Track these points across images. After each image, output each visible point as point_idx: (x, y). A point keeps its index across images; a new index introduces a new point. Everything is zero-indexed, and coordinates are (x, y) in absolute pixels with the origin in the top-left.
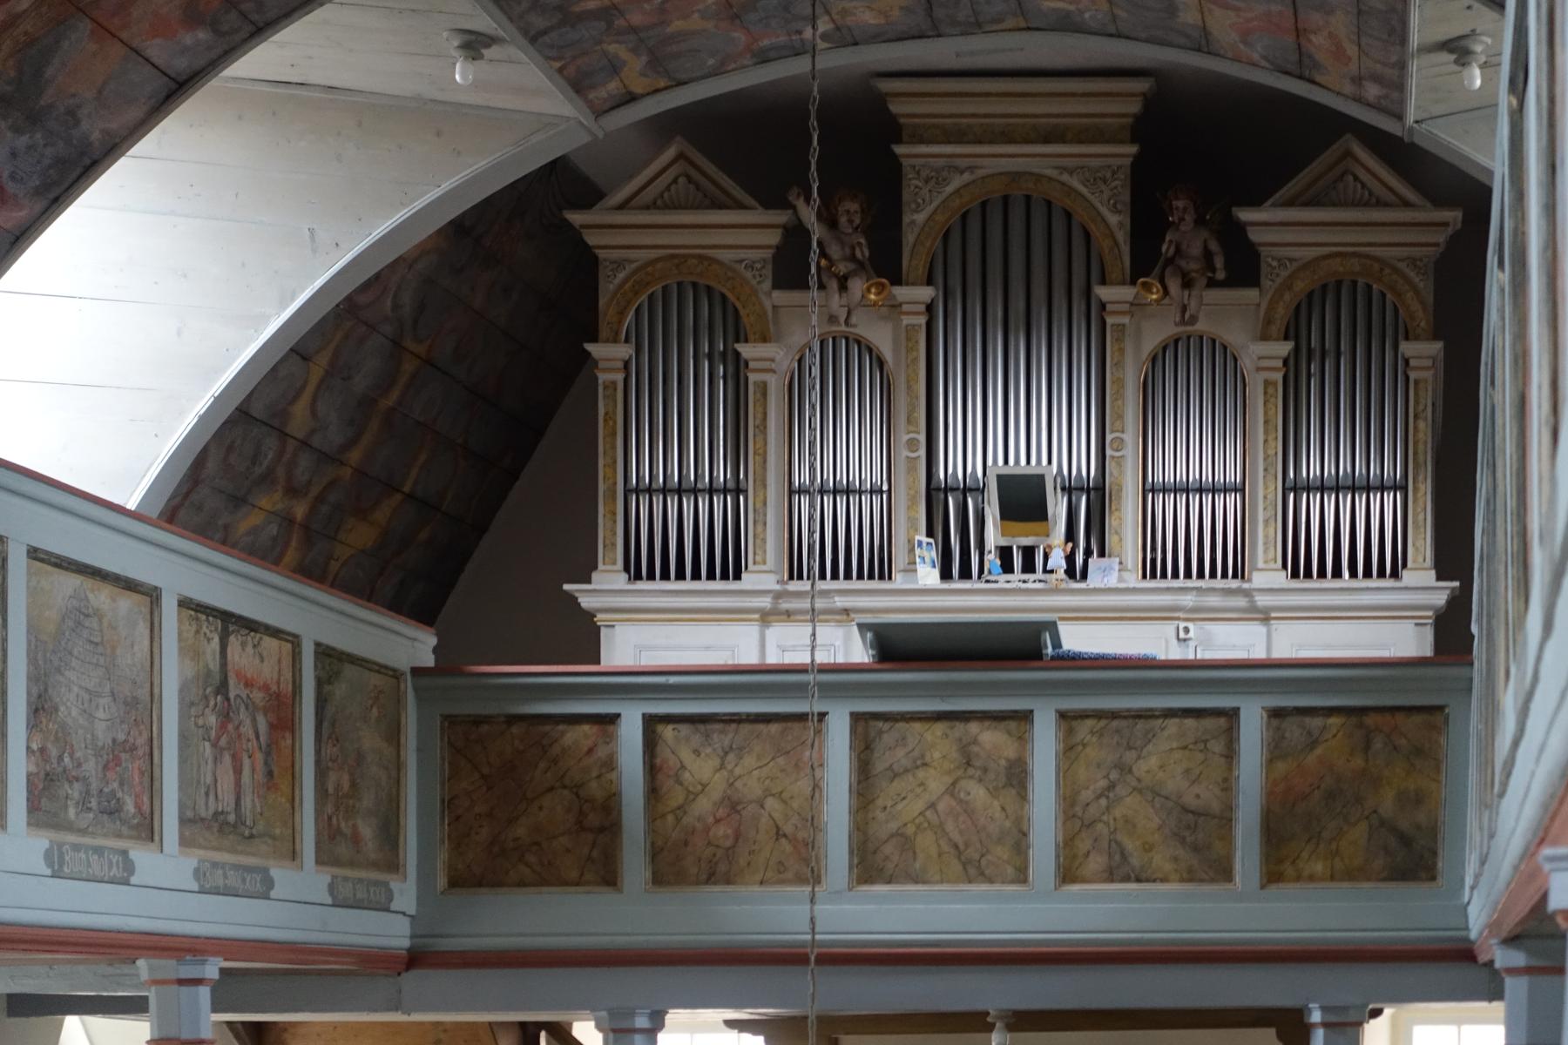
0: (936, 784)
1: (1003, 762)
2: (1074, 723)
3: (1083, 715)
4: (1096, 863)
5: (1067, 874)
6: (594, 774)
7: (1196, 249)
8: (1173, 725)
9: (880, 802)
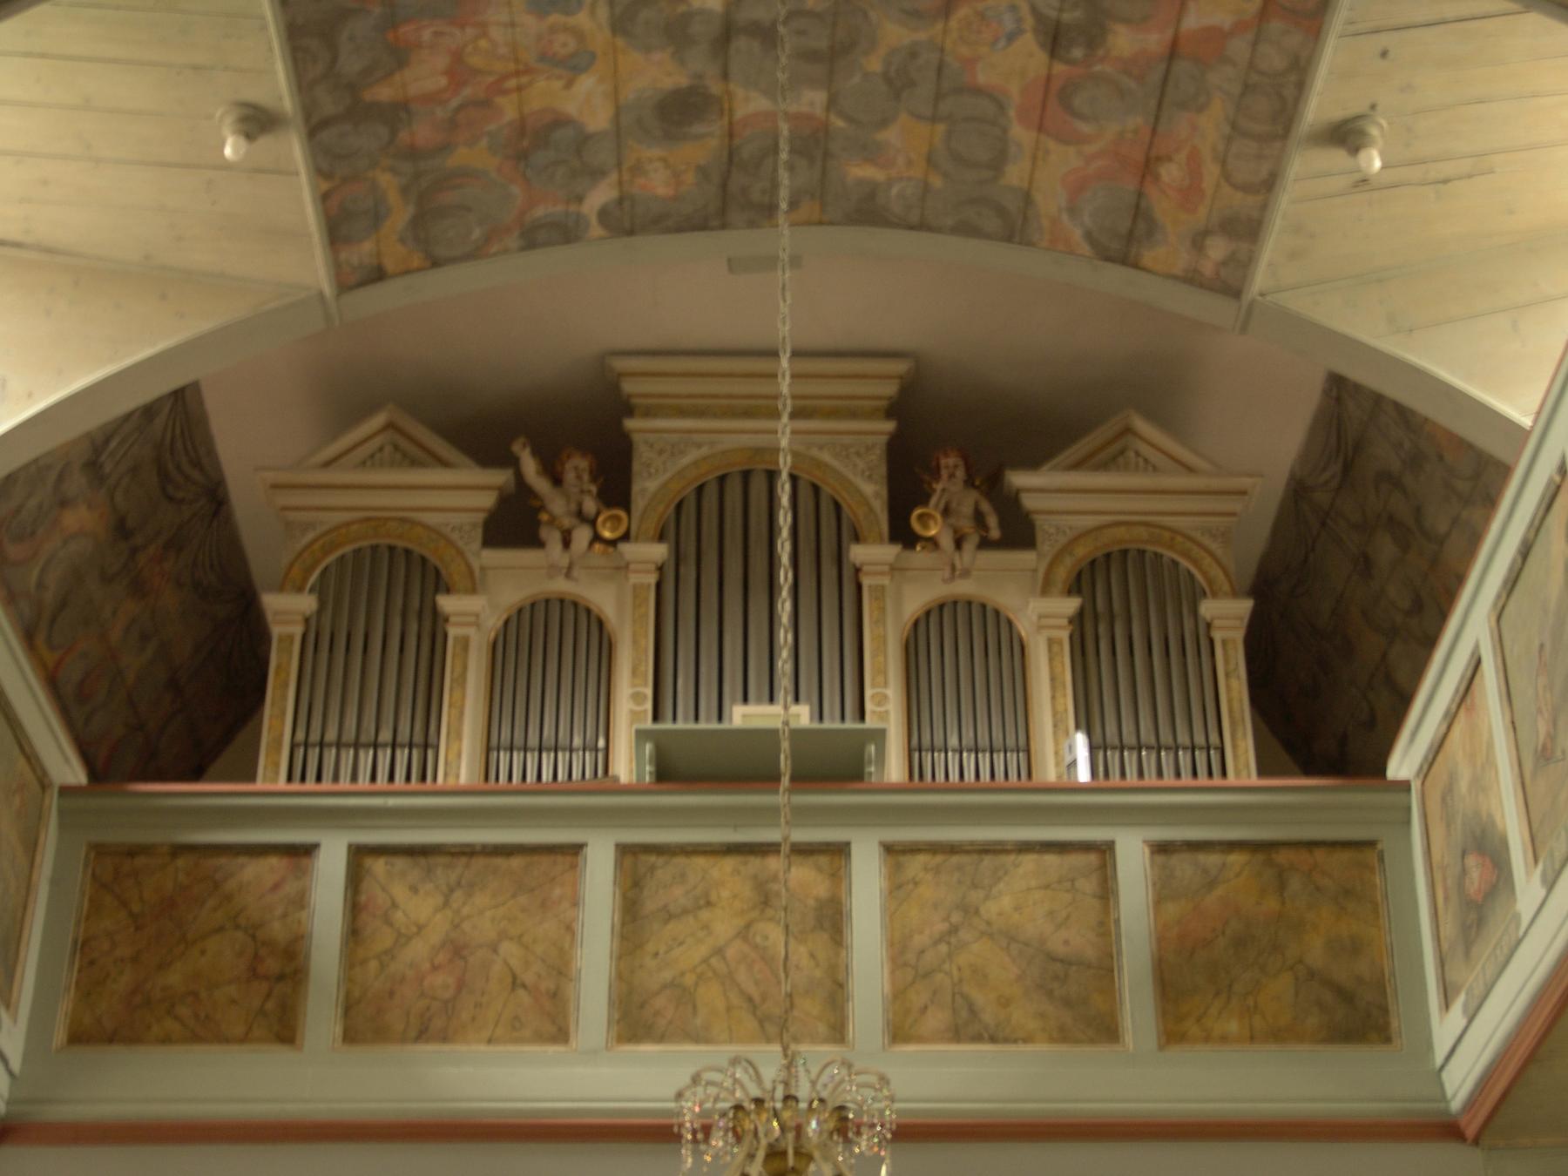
0: (723, 926)
1: (811, 902)
2: (902, 859)
3: (913, 849)
4: (937, 1019)
5: (899, 1032)
6: (279, 911)
7: (967, 509)
8: (1029, 861)
9: (650, 947)
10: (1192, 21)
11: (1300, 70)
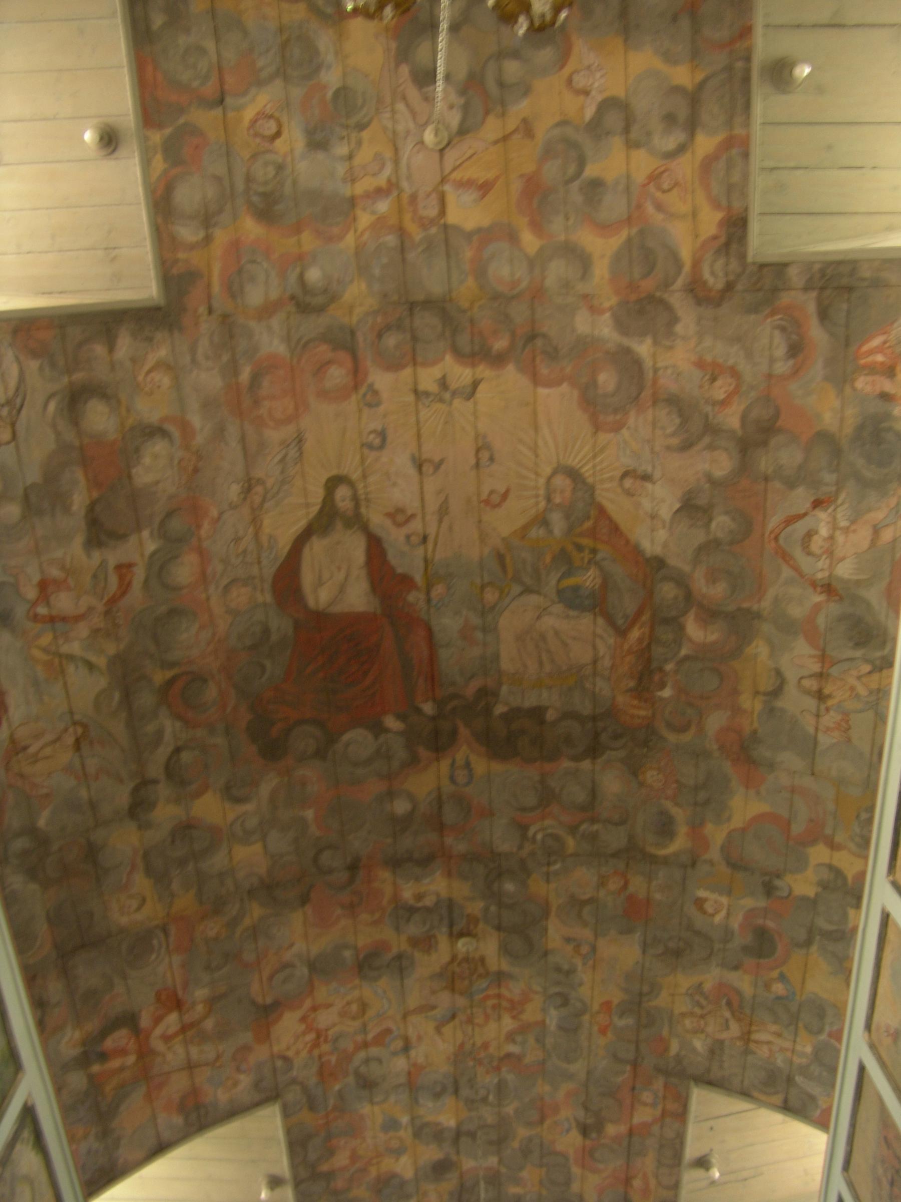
10: (636, 1120)
11: (681, 1137)
